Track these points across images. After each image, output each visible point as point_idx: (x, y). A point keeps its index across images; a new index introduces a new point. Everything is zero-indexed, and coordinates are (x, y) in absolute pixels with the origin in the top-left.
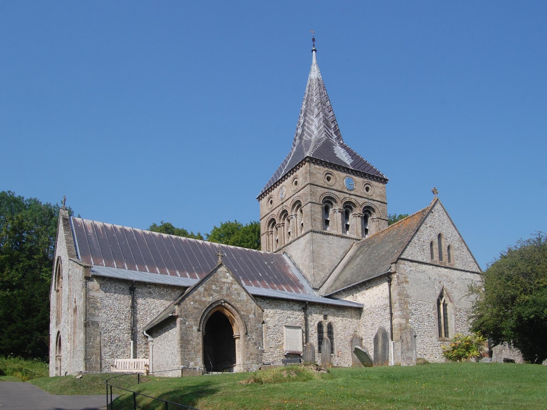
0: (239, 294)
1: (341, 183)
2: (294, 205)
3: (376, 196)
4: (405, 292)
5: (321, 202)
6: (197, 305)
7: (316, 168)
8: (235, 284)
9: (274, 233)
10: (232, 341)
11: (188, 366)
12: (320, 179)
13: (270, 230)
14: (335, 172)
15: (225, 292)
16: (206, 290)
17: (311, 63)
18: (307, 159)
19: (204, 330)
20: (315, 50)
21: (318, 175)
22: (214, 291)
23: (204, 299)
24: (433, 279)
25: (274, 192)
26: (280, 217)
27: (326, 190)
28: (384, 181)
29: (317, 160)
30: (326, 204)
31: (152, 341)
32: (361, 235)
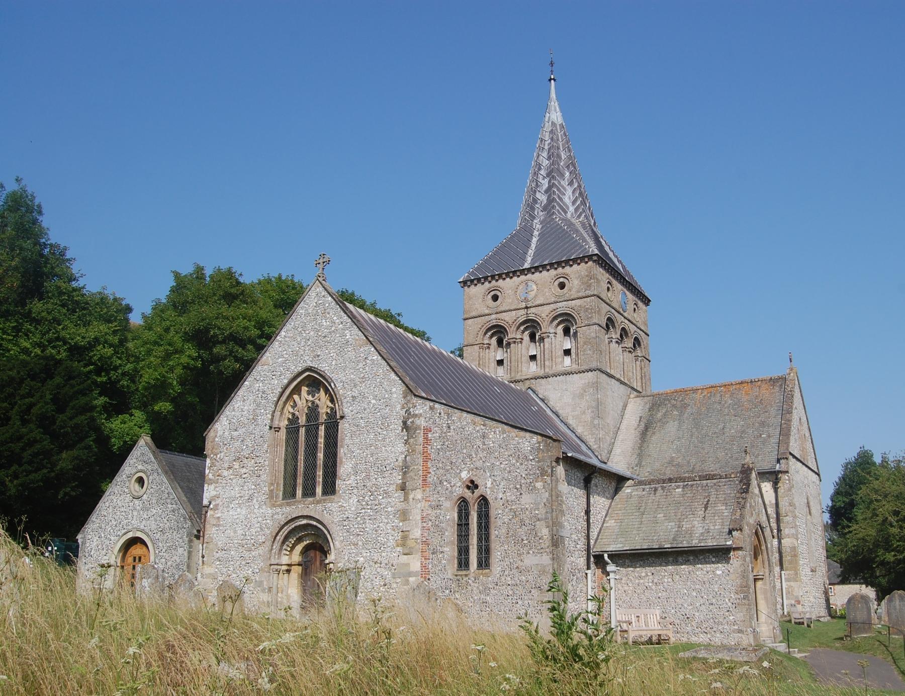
2: (555, 318)
9: (492, 347)
13: (486, 341)
17: (549, 97)
20: (554, 80)
26: (518, 328)
31: (615, 572)
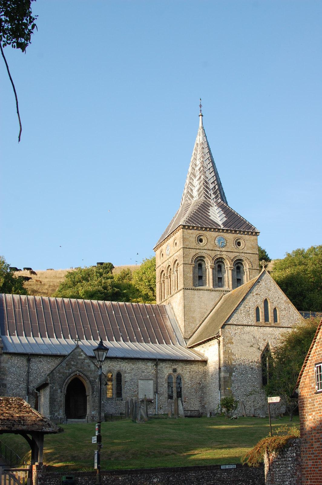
0: (89, 366)
1: (213, 243)
3: (247, 249)
4: (230, 351)
5: (193, 263)
6: (61, 375)
7: (189, 233)
8: (87, 360)
10: (85, 397)
11: (54, 415)
12: (193, 242)
14: (208, 234)
15: (79, 366)
16: (67, 365)
18: (181, 227)
19: (65, 392)
21: (191, 239)
22: (73, 365)
23: (66, 371)
24: (258, 337)
25: (164, 247)
26: (167, 270)
27: (198, 251)
28: (257, 234)
29: (189, 227)
30: (200, 262)
32: (231, 286)
